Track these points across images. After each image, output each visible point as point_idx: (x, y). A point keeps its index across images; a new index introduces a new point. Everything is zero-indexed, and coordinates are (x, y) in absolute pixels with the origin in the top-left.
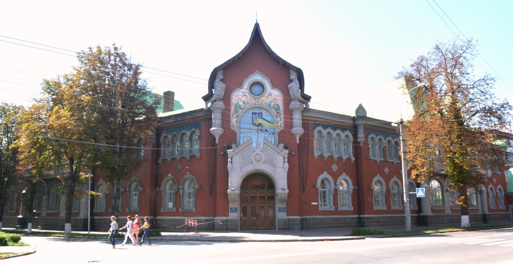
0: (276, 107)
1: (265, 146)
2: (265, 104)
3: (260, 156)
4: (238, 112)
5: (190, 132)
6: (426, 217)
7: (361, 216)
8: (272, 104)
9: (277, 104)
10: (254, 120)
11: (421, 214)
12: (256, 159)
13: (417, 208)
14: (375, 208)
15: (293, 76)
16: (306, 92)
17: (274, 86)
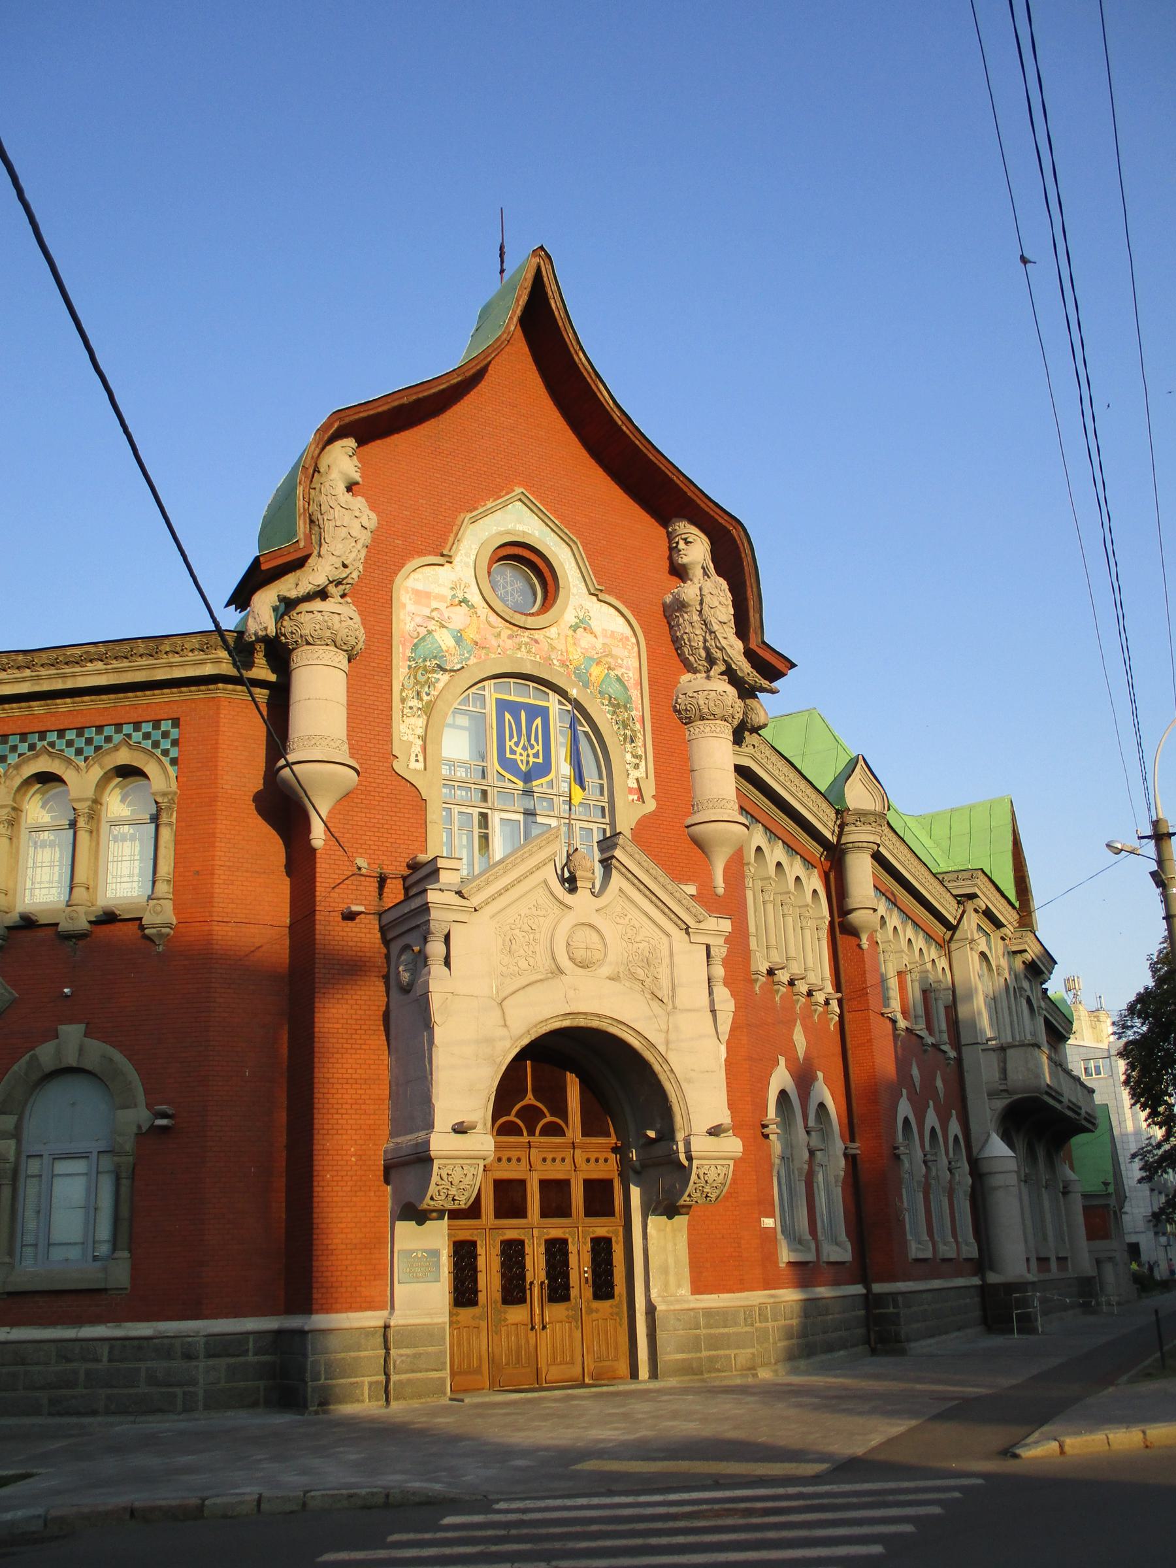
0: (614, 689)
2: (563, 664)
3: (595, 937)
4: (429, 684)
5: (96, 772)
7: (877, 1288)
9: (619, 680)
10: (508, 744)
12: (580, 954)
14: (917, 1248)
15: (696, 550)
16: (777, 633)
17: (607, 583)
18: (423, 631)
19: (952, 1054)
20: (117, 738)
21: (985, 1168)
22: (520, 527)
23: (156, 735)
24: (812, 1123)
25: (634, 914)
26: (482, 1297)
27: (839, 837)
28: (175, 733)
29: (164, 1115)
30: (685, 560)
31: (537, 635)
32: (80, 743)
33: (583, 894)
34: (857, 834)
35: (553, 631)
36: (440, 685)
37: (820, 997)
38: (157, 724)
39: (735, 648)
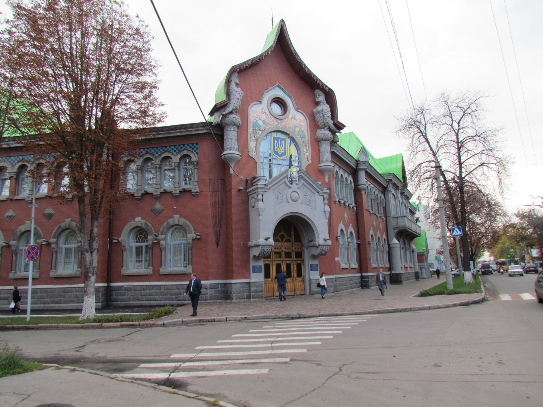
1: (302, 181)
2: (289, 128)
5: (179, 156)
6: (399, 275)
7: (364, 274)
8: (297, 129)
9: (302, 131)
10: (276, 148)
11: (393, 272)
12: (293, 198)
13: (388, 266)
15: (321, 98)
16: (341, 118)
18: (255, 121)
19: (385, 219)
20: (184, 148)
21: (391, 246)
22: (278, 93)
23: (193, 147)
24: (348, 236)
25: (306, 189)
26: (271, 276)
27: (357, 166)
28: (197, 146)
29: (199, 235)
30: (319, 100)
31: (282, 121)
32: (175, 149)
33: (294, 185)
34: (361, 166)
35: (287, 119)
36: (259, 134)
37: (351, 206)
38: (193, 144)
39: (331, 122)
